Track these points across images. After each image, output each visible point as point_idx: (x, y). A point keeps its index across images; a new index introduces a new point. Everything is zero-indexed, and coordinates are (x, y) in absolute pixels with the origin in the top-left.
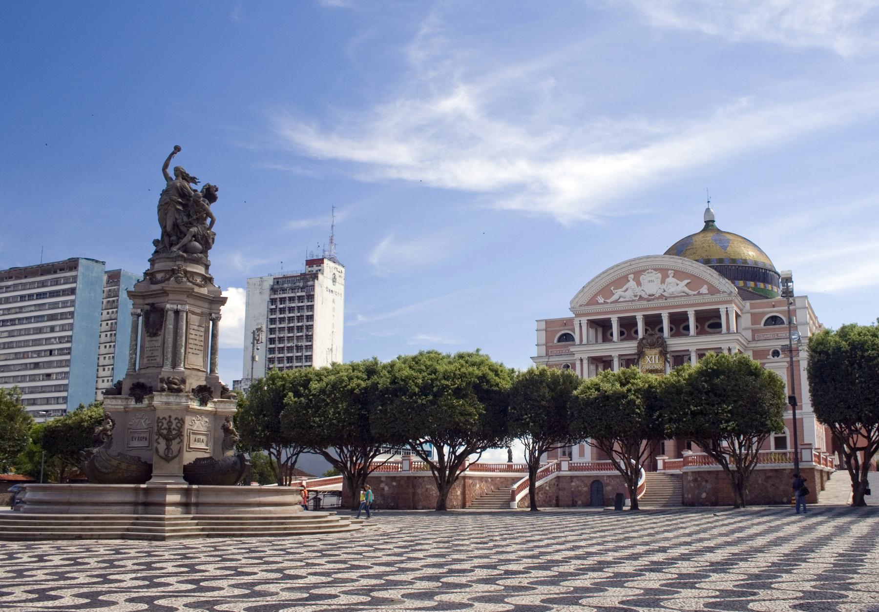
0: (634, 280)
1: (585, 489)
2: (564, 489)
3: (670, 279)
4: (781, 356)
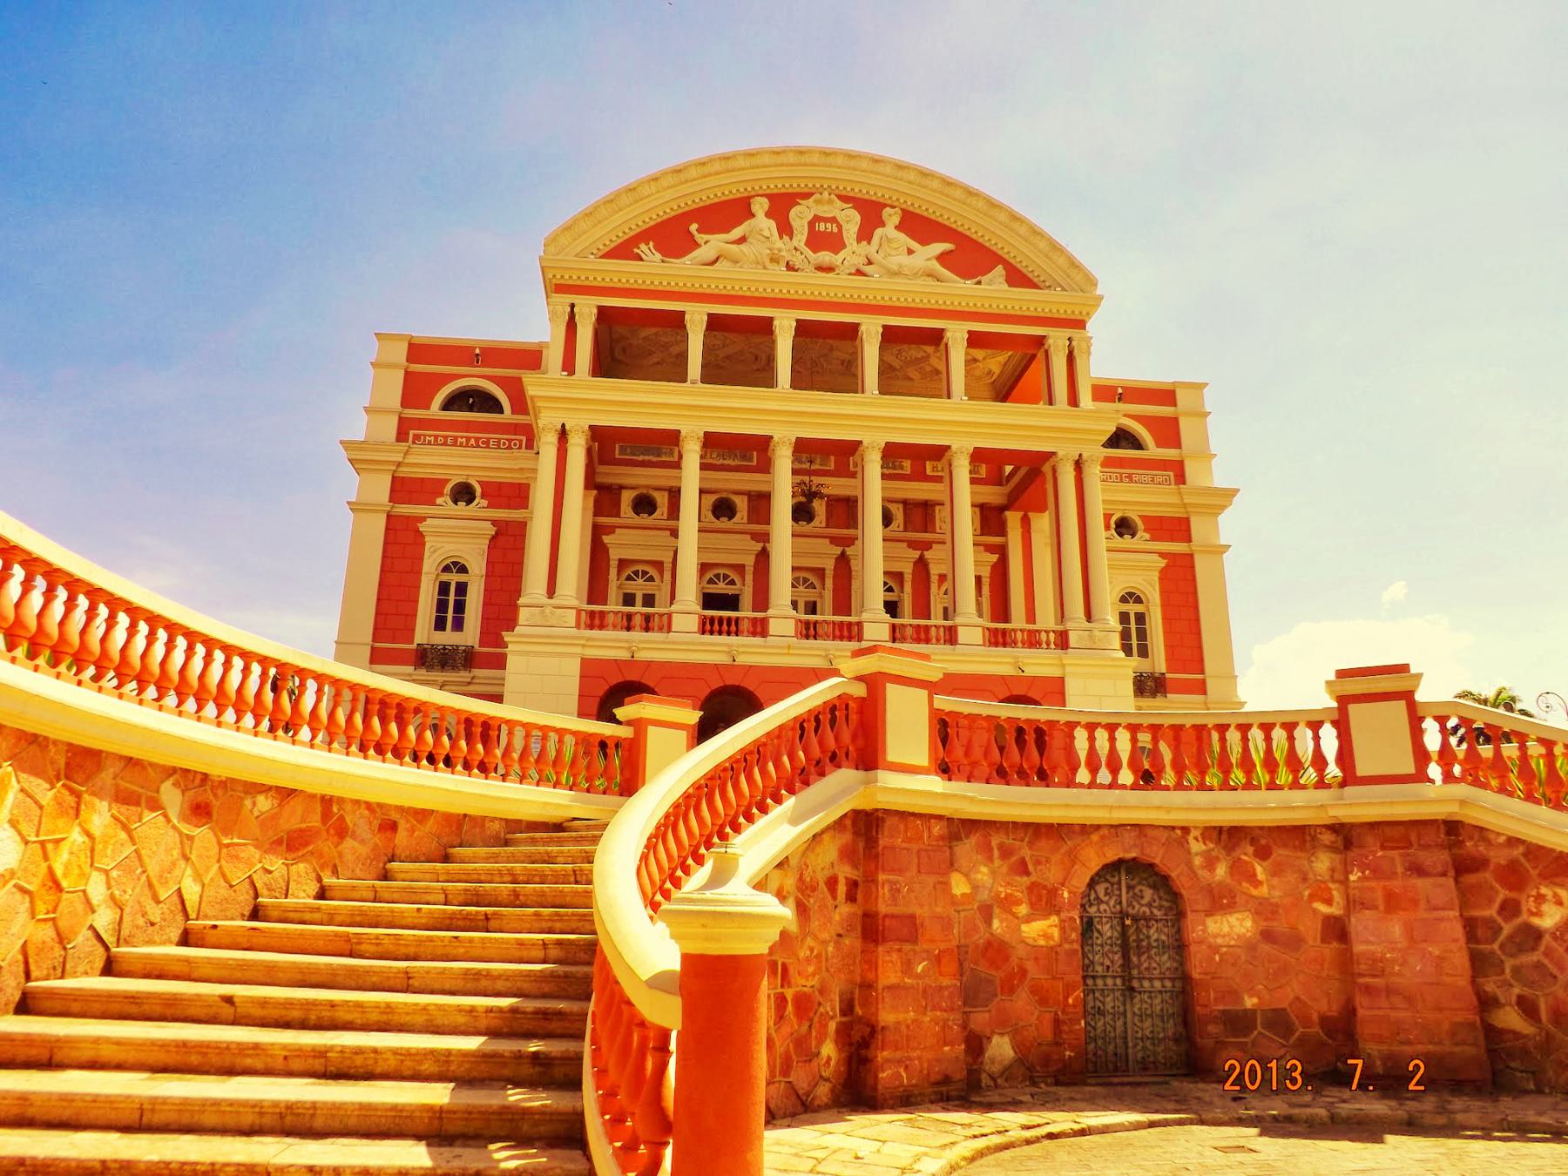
0: (768, 215)
1: (1040, 930)
2: (910, 929)
3: (889, 230)
4: (1142, 534)
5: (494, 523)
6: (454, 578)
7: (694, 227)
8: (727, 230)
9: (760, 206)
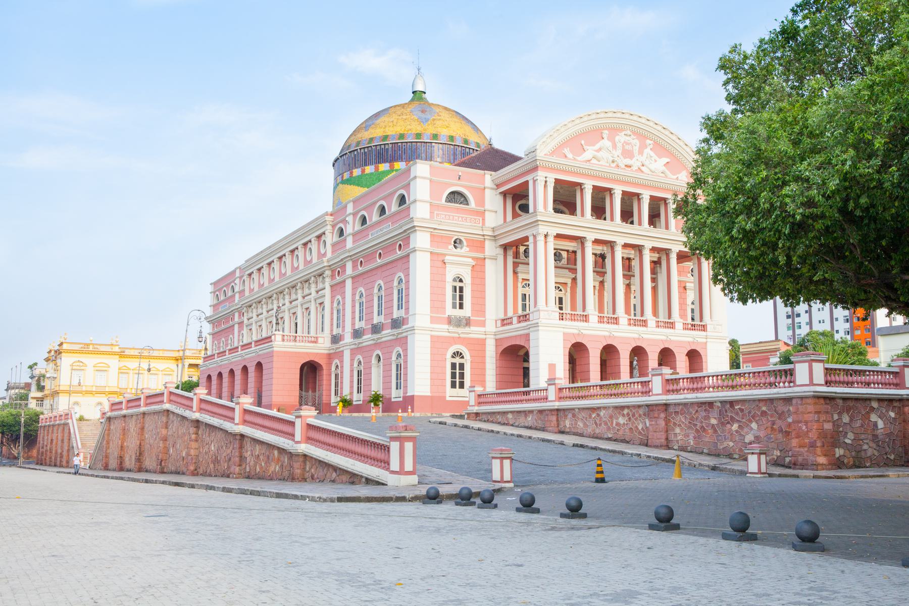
5: (473, 258)
6: (458, 284)
7: (583, 142)
8: (594, 145)
9: (606, 133)
